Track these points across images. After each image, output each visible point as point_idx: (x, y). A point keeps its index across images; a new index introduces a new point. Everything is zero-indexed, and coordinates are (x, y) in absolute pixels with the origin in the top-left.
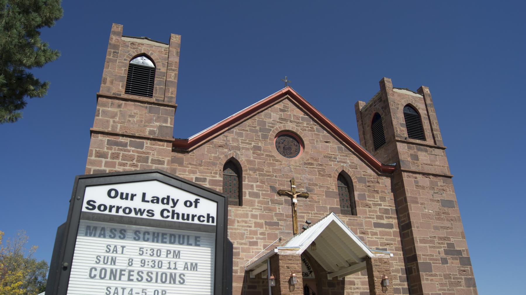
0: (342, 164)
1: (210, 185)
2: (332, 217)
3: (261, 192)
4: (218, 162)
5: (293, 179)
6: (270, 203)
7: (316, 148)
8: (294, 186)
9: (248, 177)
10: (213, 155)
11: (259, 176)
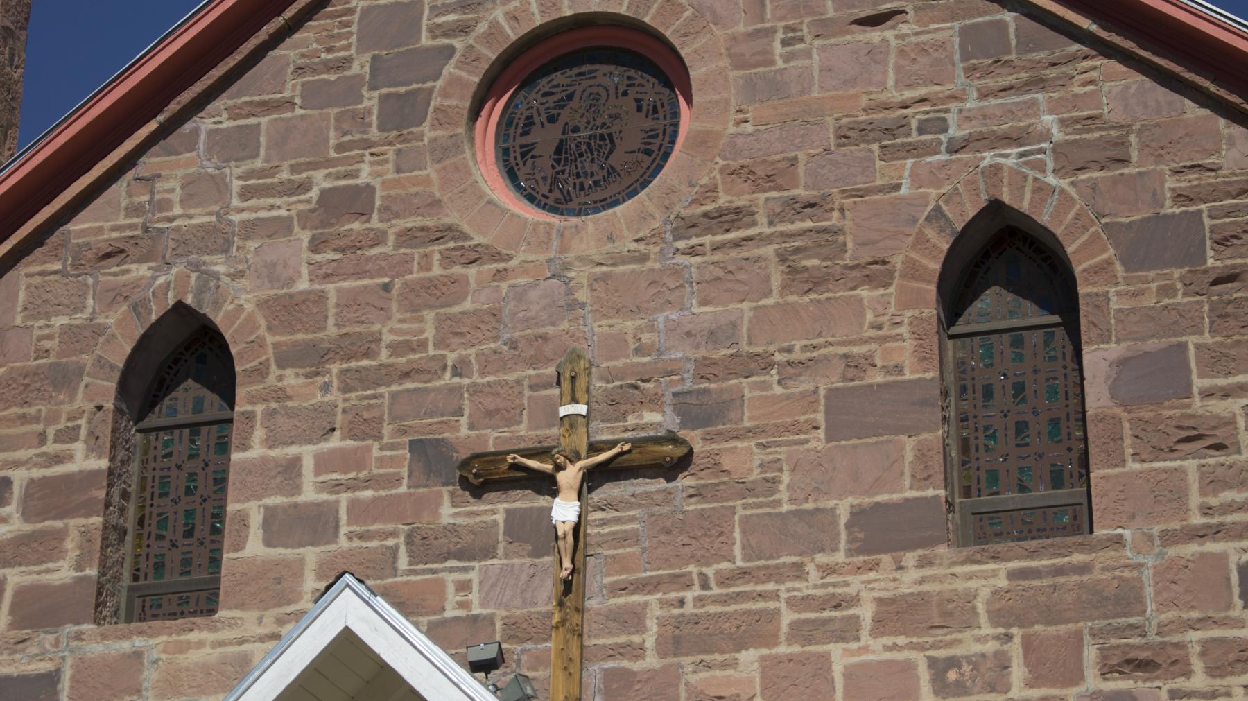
0: (988, 158)
1: (27, 516)
2: (352, 611)
3: (344, 498)
4: (87, 359)
5: (575, 356)
6: (403, 562)
7: (775, 88)
8: (582, 409)
9: (271, 414)
10: (60, 321)
11: (346, 389)
